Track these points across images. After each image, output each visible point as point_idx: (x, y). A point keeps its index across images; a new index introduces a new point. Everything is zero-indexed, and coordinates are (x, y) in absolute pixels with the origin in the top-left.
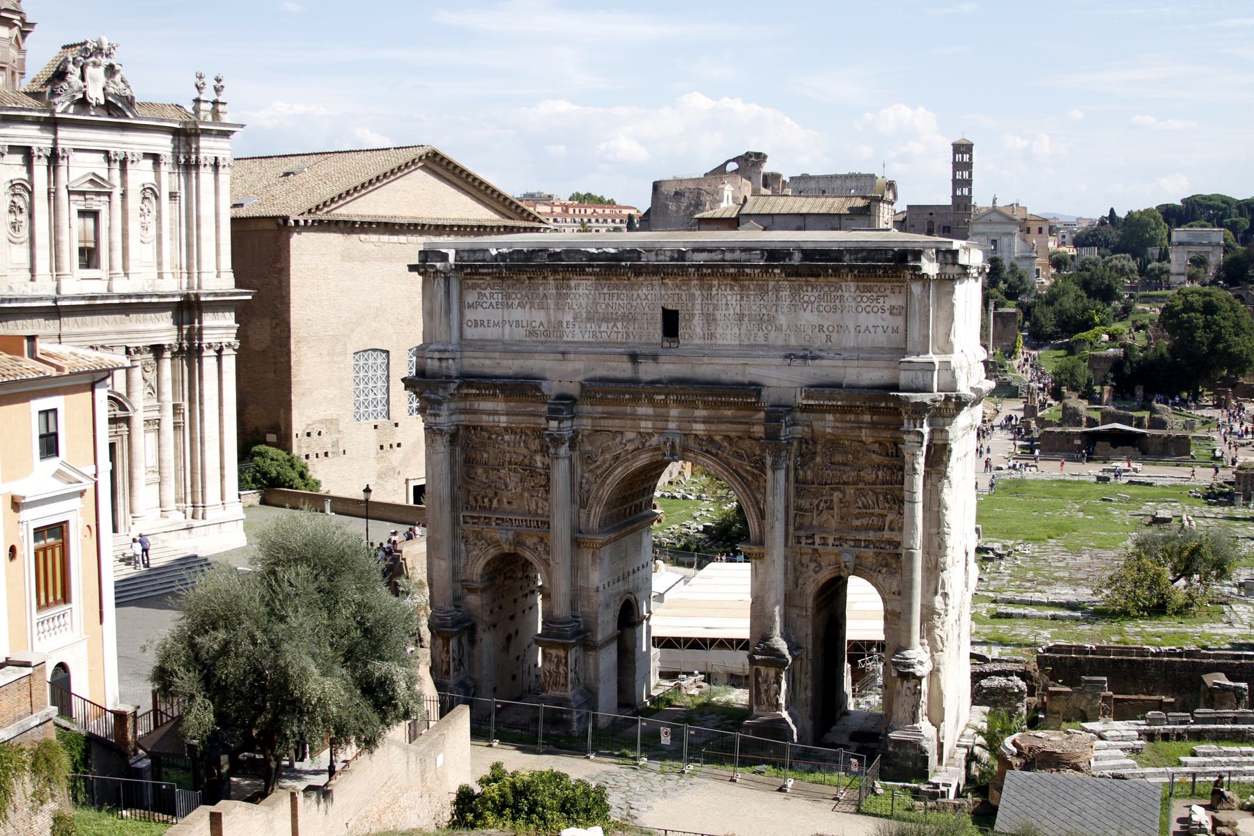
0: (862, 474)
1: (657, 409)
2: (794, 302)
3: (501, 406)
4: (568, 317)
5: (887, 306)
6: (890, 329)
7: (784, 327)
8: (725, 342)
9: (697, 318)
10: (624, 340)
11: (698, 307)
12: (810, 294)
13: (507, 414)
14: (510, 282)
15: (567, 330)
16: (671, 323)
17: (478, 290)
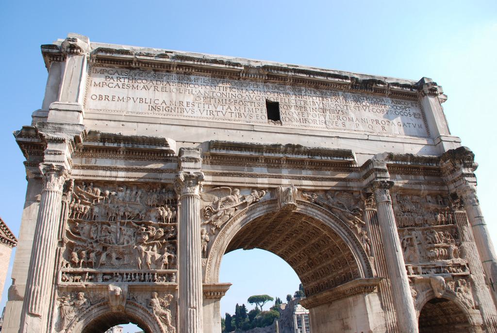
0: (425, 217)
1: (270, 169)
2: (357, 105)
3: (121, 164)
4: (190, 99)
5: (411, 113)
6: (417, 126)
7: (354, 120)
8: (316, 125)
9: (293, 110)
10: (237, 118)
11: (294, 102)
12: (366, 102)
13: (127, 170)
14: (137, 71)
15: (188, 109)
16: (273, 111)
17: (106, 74)
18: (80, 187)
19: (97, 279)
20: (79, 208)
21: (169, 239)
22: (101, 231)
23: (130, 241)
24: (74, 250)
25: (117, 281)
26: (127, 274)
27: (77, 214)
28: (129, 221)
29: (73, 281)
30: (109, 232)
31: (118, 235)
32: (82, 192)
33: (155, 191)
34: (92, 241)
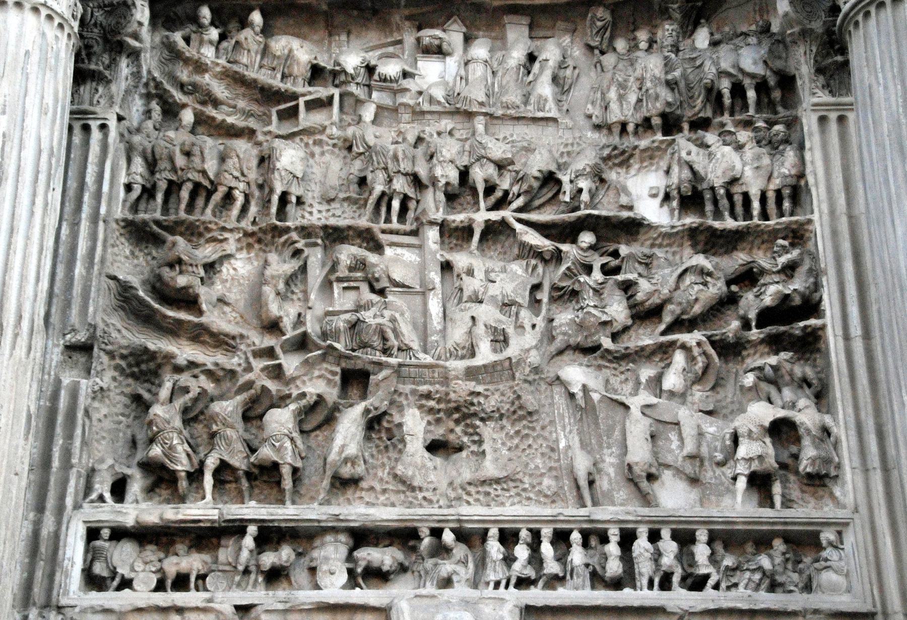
18: (187, 40)
19: (313, 570)
20: (188, 154)
21: (766, 317)
22: (327, 285)
23: (510, 331)
24: (164, 393)
25: (447, 583)
26: (508, 538)
27: (173, 188)
28: (495, 216)
29: (160, 587)
30: (373, 290)
31: (434, 306)
32: (200, 67)
33: (643, 45)
34: (269, 341)
